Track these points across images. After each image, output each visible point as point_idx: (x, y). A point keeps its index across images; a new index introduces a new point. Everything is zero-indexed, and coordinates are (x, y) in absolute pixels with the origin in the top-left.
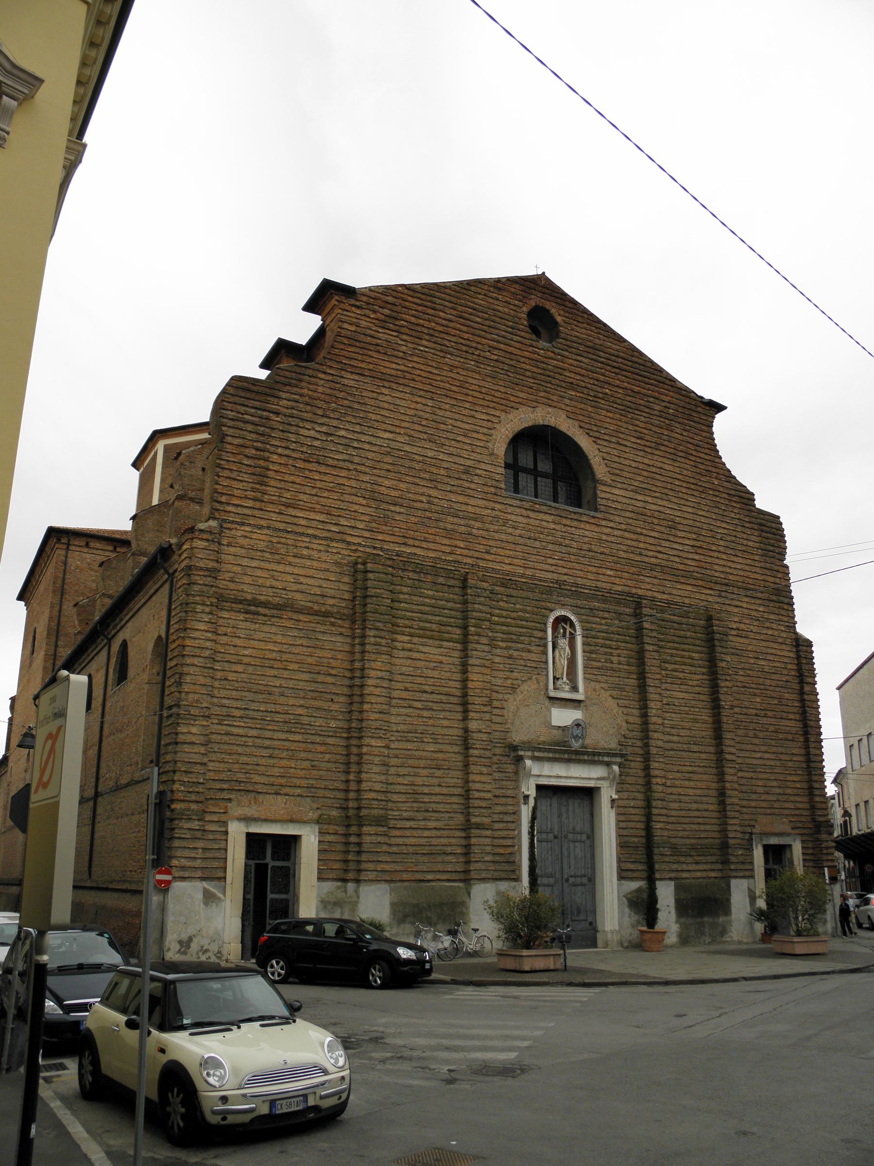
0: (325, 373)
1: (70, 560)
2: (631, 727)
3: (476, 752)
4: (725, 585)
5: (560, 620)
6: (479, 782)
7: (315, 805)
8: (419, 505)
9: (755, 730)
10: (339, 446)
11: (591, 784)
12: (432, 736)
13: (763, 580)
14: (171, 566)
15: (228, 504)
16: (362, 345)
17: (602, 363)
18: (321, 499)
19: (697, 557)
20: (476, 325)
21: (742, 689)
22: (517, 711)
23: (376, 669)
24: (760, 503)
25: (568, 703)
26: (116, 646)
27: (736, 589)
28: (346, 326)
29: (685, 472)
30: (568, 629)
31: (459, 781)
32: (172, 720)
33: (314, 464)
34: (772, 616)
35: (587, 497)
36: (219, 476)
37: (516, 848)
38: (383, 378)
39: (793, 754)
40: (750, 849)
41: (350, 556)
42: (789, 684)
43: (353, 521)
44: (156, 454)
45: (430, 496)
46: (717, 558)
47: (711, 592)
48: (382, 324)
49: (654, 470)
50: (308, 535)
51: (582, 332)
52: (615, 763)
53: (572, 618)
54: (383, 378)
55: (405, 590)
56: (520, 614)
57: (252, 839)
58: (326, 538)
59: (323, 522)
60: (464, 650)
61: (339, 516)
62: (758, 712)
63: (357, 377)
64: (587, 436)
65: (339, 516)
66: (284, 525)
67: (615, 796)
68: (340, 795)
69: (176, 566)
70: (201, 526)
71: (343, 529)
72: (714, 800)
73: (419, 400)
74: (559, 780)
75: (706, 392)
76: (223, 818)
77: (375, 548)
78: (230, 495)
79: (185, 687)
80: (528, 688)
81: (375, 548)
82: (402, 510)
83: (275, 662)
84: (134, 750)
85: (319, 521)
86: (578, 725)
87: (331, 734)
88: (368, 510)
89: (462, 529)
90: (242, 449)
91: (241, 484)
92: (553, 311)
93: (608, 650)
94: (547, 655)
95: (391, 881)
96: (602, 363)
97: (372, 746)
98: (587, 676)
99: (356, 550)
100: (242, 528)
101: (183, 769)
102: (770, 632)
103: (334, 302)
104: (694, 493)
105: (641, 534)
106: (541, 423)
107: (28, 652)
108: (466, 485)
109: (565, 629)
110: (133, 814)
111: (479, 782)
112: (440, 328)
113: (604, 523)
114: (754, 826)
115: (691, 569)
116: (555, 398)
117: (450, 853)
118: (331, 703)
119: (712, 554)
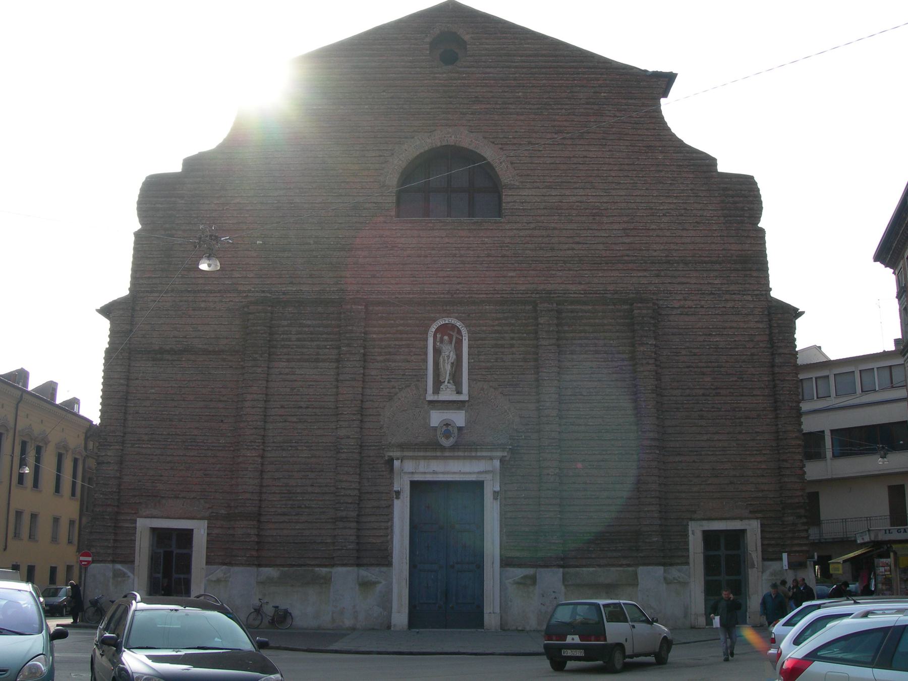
3: (344, 456)
5: (443, 329)
6: (346, 481)
9: (701, 410)
11: (473, 478)
12: (306, 445)
13: (724, 250)
21: (686, 370)
24: (723, 167)
30: (455, 334)
34: (732, 288)
37: (389, 537)
39: (756, 432)
41: (242, 302)
42: (755, 357)
43: (244, 272)
45: (317, 237)
47: (645, 274)
49: (575, 160)
50: (204, 291)
52: (491, 458)
53: (458, 324)
55: (285, 323)
56: (399, 328)
58: (219, 291)
61: (232, 270)
65: (232, 270)
66: (186, 286)
67: (497, 489)
74: (435, 476)
77: (263, 292)
81: (263, 292)
86: (447, 425)
93: (501, 350)
96: (516, 67)
97: (247, 456)
99: (247, 296)
100: (152, 295)
102: (729, 305)
106: (439, 144)
109: (451, 337)
111: (346, 481)
118: (221, 424)
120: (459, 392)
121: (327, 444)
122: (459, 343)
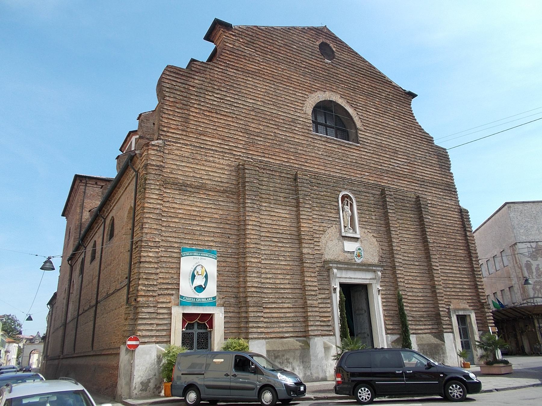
0: (218, 68)
1: (87, 191)
2: (384, 252)
4: (423, 182)
5: (343, 197)
7: (221, 296)
8: (270, 137)
10: (227, 105)
12: (284, 256)
14: (136, 167)
15: (168, 132)
16: (237, 55)
17: (356, 72)
18: (219, 132)
19: (408, 168)
20: (294, 50)
22: (326, 243)
23: (252, 219)
24: (436, 143)
25: (352, 239)
26: (108, 222)
27: (428, 184)
28: (228, 44)
29: (399, 126)
30: (349, 201)
31: (299, 281)
32: (137, 249)
33: (214, 114)
35: (352, 137)
36: (162, 117)
38: (248, 72)
40: (450, 317)
44: (131, 143)
46: (418, 168)
48: (247, 44)
51: (345, 56)
52: (378, 270)
53: (351, 195)
54: (248, 72)
57: (186, 317)
59: (220, 143)
60: (298, 211)
62: (445, 246)
63: (235, 71)
64: (351, 107)
68: (235, 290)
69: (140, 166)
70: (153, 143)
71: (231, 148)
72: (429, 291)
73: (267, 84)
74: (350, 280)
75: (407, 88)
76: (169, 305)
78: (169, 127)
79: (146, 231)
80: (332, 231)
82: (261, 139)
83: (197, 217)
84: (117, 273)
85: (218, 143)
86: (359, 249)
87: (229, 256)
88: (244, 139)
89: (292, 150)
90: (175, 104)
91: (175, 122)
92: (331, 45)
94: (339, 214)
95: (266, 338)
96: (356, 72)
98: (361, 226)
101: (144, 277)
103: (221, 32)
104: (404, 136)
105: (381, 155)
106: (329, 99)
107: (67, 240)
108: (294, 128)
110: (116, 309)
112: (276, 50)
113: (362, 149)
114: (450, 305)
115: (406, 173)
116: (334, 87)
117: (297, 321)
118: (228, 239)
119: (416, 166)
120: (356, 233)
121: (295, 257)
122: (351, 205)
